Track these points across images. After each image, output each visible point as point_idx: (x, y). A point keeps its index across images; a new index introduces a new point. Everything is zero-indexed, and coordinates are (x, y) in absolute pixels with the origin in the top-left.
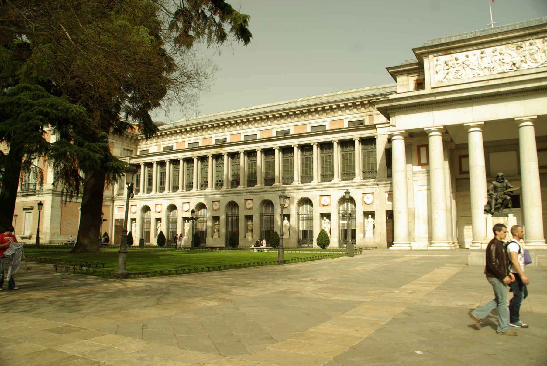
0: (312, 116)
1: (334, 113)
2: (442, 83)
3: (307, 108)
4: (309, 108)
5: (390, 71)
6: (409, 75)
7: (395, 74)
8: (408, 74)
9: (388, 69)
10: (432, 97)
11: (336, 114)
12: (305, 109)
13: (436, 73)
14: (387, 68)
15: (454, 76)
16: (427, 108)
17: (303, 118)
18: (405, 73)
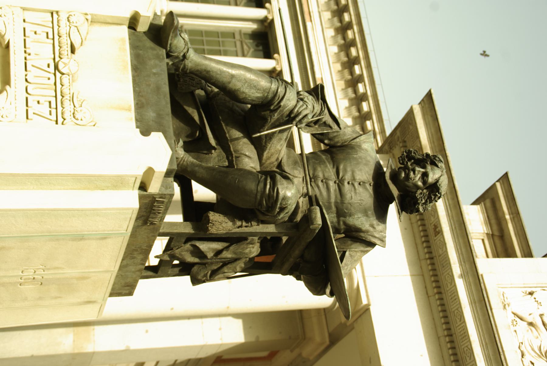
0: (332, 37)
1: (343, 89)
2: (502, 306)
3: (354, 22)
4: (355, 28)
5: (498, 185)
6: (488, 239)
7: (488, 202)
8: (491, 236)
9: (505, 179)
10: (461, 264)
11: (340, 95)
12: (353, 18)
13: (529, 290)
14: (506, 175)
15: (526, 343)
16: (419, 259)
17: (327, 15)
18: (495, 227)
